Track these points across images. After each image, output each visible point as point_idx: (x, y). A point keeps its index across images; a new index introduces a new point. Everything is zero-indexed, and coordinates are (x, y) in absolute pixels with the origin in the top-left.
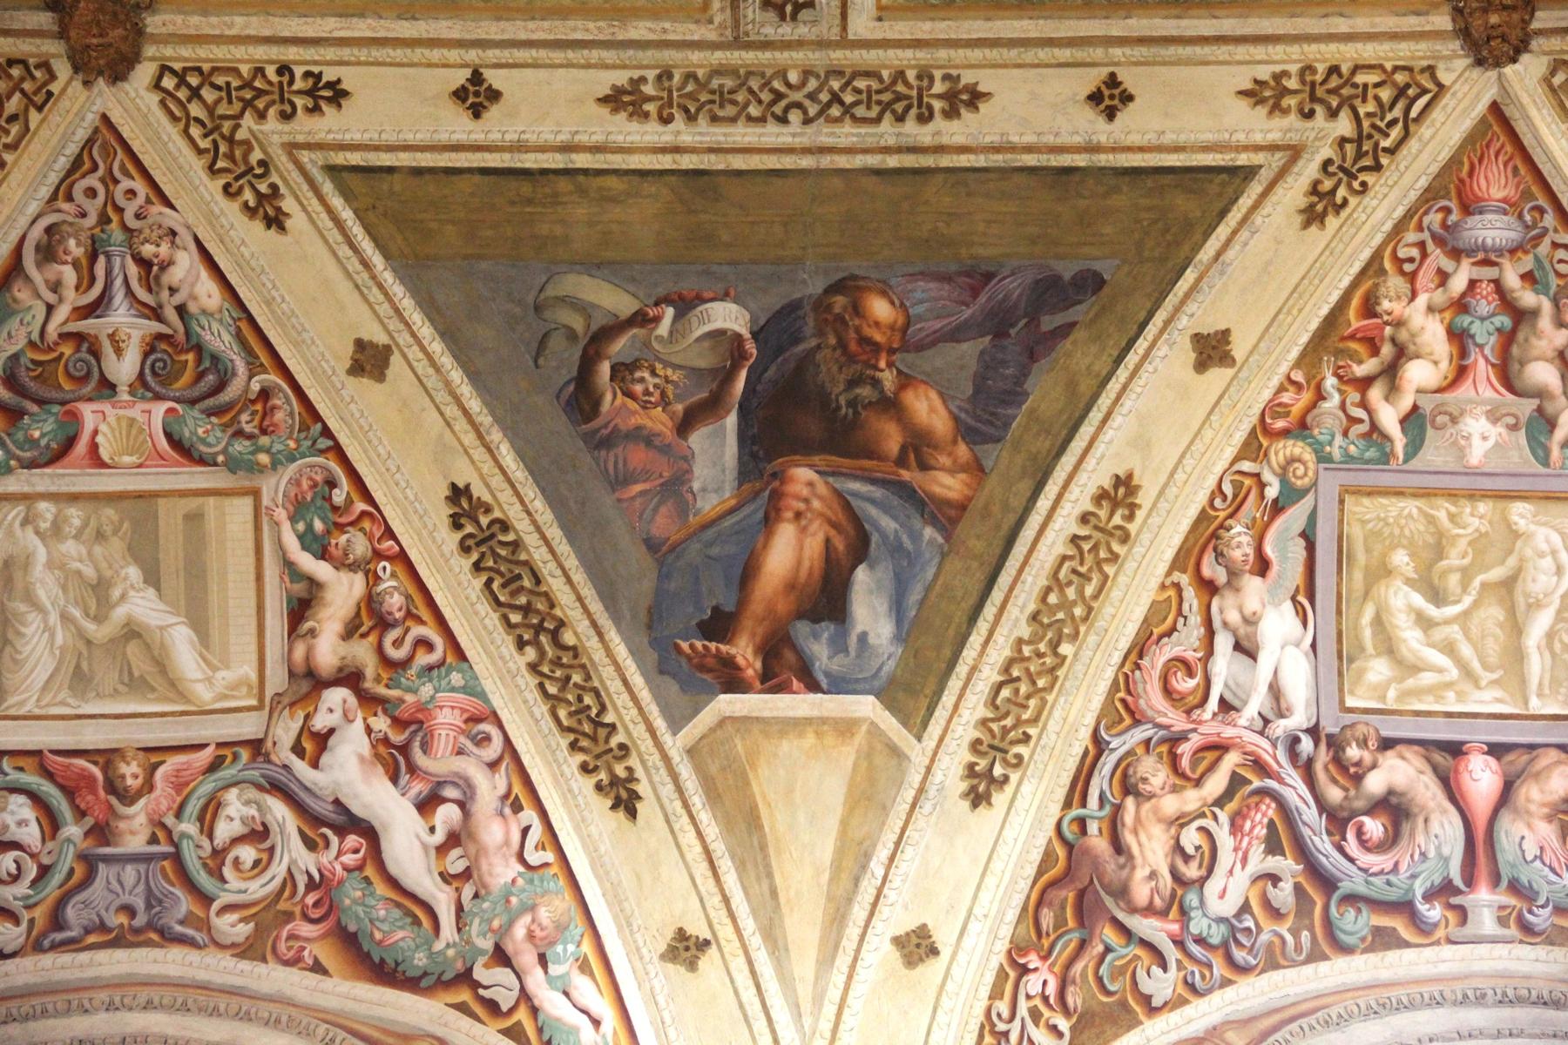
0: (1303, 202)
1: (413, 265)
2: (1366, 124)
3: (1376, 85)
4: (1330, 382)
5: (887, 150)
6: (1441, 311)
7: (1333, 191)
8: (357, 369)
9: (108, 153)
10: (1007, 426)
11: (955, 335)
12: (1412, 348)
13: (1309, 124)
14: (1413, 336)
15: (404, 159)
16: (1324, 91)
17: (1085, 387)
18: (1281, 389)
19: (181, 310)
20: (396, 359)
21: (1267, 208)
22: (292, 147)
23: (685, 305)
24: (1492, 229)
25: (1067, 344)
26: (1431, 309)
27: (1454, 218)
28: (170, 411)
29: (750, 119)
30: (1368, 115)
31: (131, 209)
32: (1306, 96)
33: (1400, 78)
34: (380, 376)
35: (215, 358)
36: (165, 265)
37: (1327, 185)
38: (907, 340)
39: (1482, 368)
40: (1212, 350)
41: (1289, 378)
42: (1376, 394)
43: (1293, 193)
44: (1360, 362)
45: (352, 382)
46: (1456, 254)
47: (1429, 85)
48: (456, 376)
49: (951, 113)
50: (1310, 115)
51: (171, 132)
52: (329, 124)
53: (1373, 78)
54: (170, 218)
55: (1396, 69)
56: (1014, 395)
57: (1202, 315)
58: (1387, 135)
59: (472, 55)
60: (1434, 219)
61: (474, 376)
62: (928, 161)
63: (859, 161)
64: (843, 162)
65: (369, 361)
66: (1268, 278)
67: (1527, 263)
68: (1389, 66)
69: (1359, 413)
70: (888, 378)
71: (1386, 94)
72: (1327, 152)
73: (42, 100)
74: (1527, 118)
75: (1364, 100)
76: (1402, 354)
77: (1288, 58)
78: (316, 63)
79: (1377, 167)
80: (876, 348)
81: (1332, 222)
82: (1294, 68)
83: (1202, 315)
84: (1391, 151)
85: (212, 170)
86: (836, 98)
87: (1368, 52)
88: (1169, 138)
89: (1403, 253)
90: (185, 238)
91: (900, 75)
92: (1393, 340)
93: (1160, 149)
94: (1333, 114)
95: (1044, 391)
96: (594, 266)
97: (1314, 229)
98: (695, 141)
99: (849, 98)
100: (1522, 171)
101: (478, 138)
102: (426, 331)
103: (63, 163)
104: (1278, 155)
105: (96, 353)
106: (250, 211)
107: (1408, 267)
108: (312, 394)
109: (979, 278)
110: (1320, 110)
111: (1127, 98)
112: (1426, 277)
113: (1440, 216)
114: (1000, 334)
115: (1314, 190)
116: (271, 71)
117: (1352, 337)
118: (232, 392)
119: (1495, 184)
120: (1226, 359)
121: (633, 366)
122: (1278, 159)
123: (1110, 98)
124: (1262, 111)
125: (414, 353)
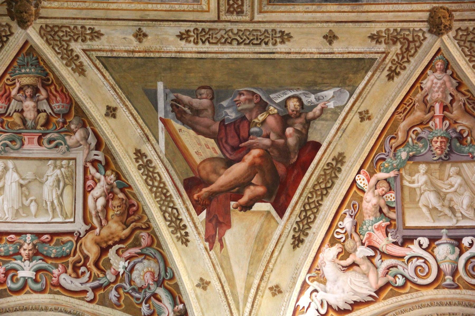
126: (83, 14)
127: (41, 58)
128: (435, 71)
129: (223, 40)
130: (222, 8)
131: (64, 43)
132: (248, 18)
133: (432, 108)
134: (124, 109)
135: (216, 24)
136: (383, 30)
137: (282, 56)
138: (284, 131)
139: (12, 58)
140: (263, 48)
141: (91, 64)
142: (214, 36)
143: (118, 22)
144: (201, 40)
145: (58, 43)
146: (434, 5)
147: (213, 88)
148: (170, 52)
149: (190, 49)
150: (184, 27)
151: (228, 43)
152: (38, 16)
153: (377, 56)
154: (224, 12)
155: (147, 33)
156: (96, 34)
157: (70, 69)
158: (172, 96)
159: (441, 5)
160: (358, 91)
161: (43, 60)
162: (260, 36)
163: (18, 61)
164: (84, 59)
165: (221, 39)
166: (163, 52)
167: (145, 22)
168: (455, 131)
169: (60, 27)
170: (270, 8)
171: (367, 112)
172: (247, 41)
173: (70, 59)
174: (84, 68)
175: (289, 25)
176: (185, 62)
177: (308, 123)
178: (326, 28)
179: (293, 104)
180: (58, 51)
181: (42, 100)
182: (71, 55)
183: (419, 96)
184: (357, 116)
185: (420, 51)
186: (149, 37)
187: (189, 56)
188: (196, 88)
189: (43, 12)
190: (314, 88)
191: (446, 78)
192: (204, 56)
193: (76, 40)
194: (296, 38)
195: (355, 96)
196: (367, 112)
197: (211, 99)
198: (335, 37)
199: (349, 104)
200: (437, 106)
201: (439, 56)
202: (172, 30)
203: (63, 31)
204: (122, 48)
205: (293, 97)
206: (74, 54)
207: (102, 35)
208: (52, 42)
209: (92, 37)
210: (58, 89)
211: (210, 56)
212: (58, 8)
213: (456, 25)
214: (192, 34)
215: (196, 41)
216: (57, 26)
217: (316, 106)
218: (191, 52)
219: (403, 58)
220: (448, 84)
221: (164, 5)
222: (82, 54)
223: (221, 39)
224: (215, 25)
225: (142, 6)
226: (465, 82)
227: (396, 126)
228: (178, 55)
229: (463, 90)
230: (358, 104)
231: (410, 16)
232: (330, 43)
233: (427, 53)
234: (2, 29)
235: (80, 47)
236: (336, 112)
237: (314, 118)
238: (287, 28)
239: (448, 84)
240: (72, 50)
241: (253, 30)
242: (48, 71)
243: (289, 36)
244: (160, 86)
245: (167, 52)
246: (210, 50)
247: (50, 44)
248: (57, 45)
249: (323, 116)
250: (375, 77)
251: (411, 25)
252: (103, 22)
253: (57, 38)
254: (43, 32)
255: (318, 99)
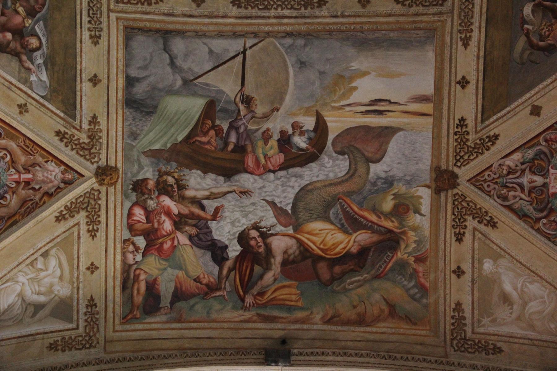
1: (509, 99)
8: (538, 115)
9: (478, 181)
15: (480, 102)
19: (522, 164)
20: (536, 104)
22: (476, 132)
23: (524, 21)
28: (552, 168)
29: (473, 7)
31: (493, 176)
34: (541, 108)
35: (536, 155)
36: (509, 167)
45: (542, 116)
48: (541, 86)
51: (472, 164)
52: (470, 122)
54: (496, 165)
59: (453, 84)
61: (542, 81)
65: (536, 111)
73: (463, 197)
78: (454, 125)
85: (482, 153)
90: (501, 162)
96: (512, 48)
98: (478, 22)
101: (474, 82)
102: (528, 95)
103: (480, 193)
105: (535, 188)
106: (494, 144)
108: (545, 127)
116: (456, 137)
118: (546, 150)
121: (540, 35)
125: (534, 98)
128: (63, 173)
132: (112, 7)
133: (27, 171)
136: (101, 127)
137: (78, 35)
138: (9, 30)
140: (85, 19)
146: (121, 170)
153: (78, 122)
159: (120, 176)
160: (46, 103)
162: (97, 17)
168: (6, 192)
170: (121, 28)
171: (27, 111)
172: (91, 5)
175: (106, 43)
177: (16, 55)
178: (103, 76)
179: (33, 42)
183: (40, 159)
184: (23, 102)
185: (82, 159)
190: (50, 63)
191: (56, 183)
194: (95, 49)
195: (42, 100)
196: (27, 111)
198: (95, 85)
199: (34, 95)
200: (30, 176)
201: (76, 176)
205: (41, 43)
213: (103, 189)
217: (33, 64)
219: (76, 145)
220: (50, 185)
226: (53, 199)
227: (12, 138)
229: (45, 198)
230: (34, 103)
231: (112, 150)
232: (89, 80)
233: (80, 164)
236: (26, 82)
237: (21, 61)
238: (103, 41)
239: (50, 185)
241: (101, 11)
243: (96, 43)
249: (23, 70)
250: (59, 120)
251: (104, 151)
255: (39, 66)
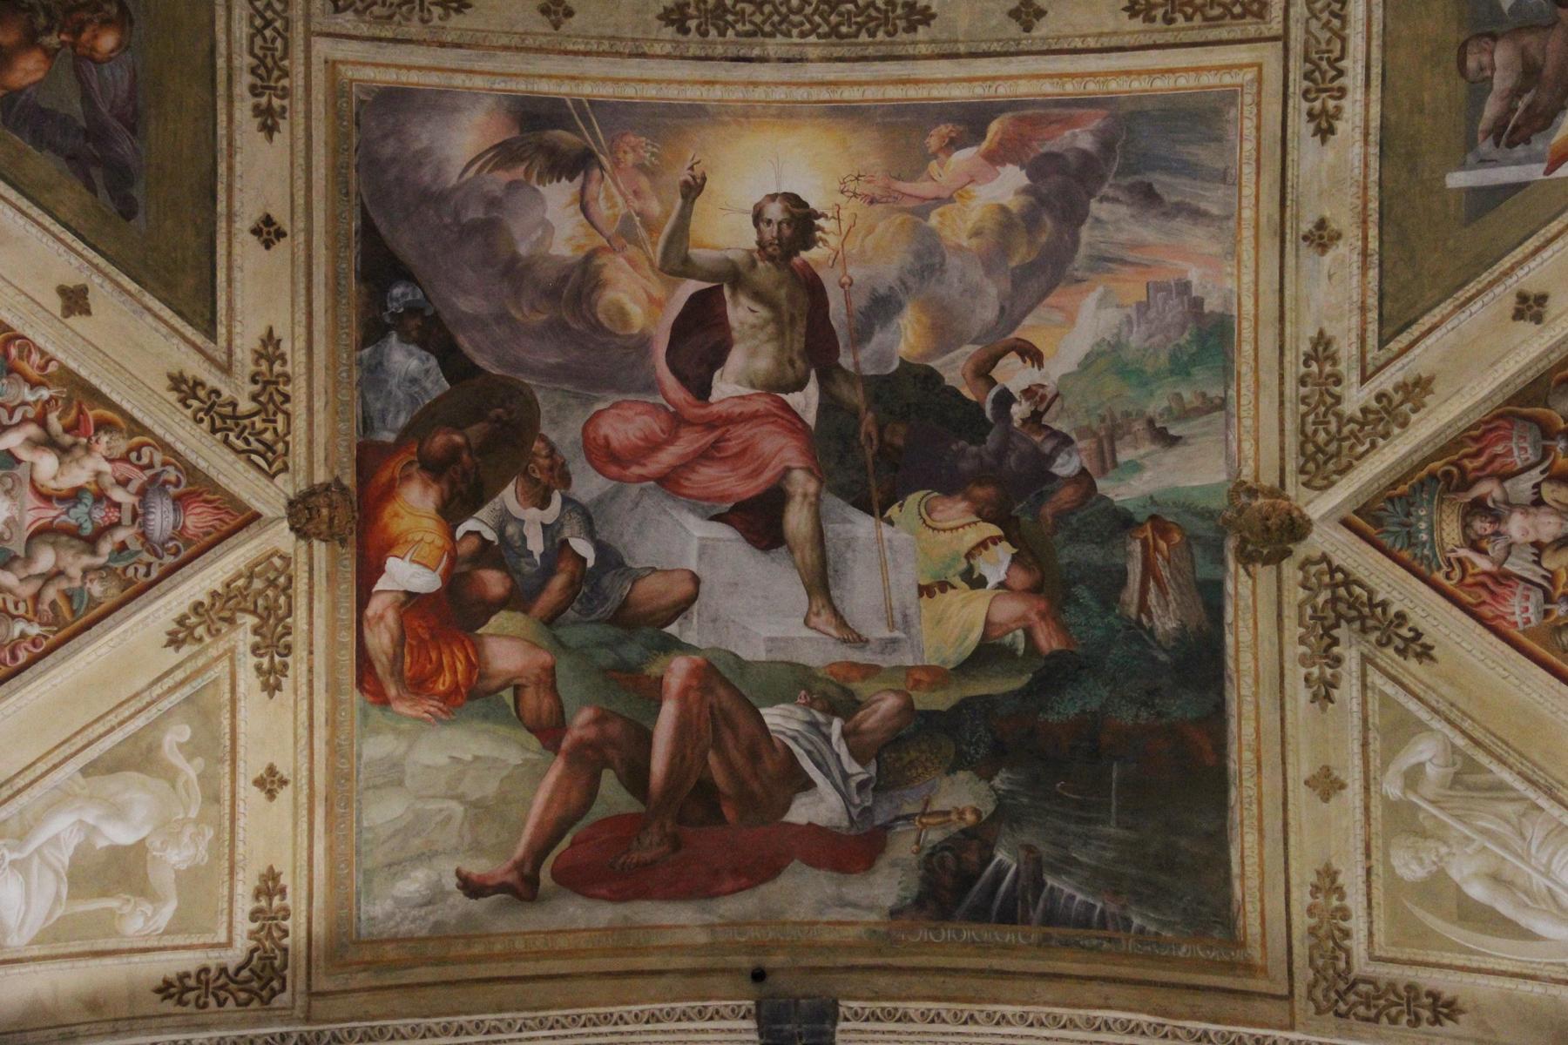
0: (188, 374)
2: (247, 422)
3: (275, 430)
4: (45, 394)
5: (229, 59)
6: (96, 482)
7: (196, 397)
10: (16, 130)
11: (87, 97)
12: (68, 459)
13: (247, 379)
14: (77, 461)
16: (271, 390)
17: (46, 197)
18: (43, 353)
21: (184, 347)
24: (161, 519)
25: (79, 186)
26: (98, 474)
27: (172, 490)
30: (253, 424)
32: (268, 377)
33: (280, 447)
37: (202, 393)
38: (83, 59)
39: (50, 513)
40: (75, 300)
41: (52, 359)
42: (33, 430)
43: (195, 367)
44: (60, 418)
46: (142, 493)
47: (275, 468)
49: (258, 112)
50: (254, 381)
53: (280, 426)
55: (287, 444)
56: (39, 140)
57: (102, 294)
58: (238, 438)
60: (171, 474)
62: (221, 89)
63: (221, 37)
64: (220, 25)
66: (129, 348)
67: (134, 545)
68: (289, 438)
69: (17, 417)
70: (52, 40)
71: (268, 436)
72: (226, 393)
74: (252, 538)
75: (264, 421)
76: (63, 451)
77: (296, 363)
79: (214, 431)
80: (77, 33)
81: (173, 397)
82: (288, 369)
83: (102, 294)
84: (226, 441)
86: (268, 23)
87: (300, 424)
88: (237, 275)
89: (146, 451)
91: (285, 74)
92: (75, 444)
93: (230, 268)
94: (254, 398)
95: (43, 165)
97: (168, 382)
99: (268, 33)
100: (208, 539)
104: (224, 357)
107: (133, 455)
109: (133, 124)
110: (257, 388)
111: (268, 245)
112: (124, 469)
113: (173, 478)
114: (87, 134)
115: (198, 383)
117: (81, 412)
119: (197, 520)
120: (68, 311)
122: (222, 357)
123: (268, 232)
124: (257, 345)
126: (1270, 380)
127: (1387, 488)
129: (1336, 23)
130: (1252, 31)
131: (1346, 431)
134: (1520, 273)
135: (1292, 44)
139: (1388, 562)
141: (1398, 364)
142: (1323, 46)
143: (1287, 293)
144: (1333, 79)
145: (1346, 444)
147: (1462, 39)
148: (1366, 157)
149: (1357, 109)
150: (1300, 126)
151: (1342, 9)
152: (1278, 492)
154: (1263, 27)
155: (1316, 219)
156: (1320, 349)
157: (1414, 417)
158: (1486, 146)
161: (1394, 485)
163: (1398, 547)
164: (1387, 381)
165: (1331, 30)
166: (1365, 177)
167: (1288, 224)
169: (1305, 438)
173: (1385, 416)
174: (1410, 380)
176: (1393, 118)
180: (1367, 445)
181: (1505, 492)
182: (1378, 412)
186: (1327, 214)
187: (1375, 110)
188: (1462, 82)
189: (1269, 479)
192: (1376, 70)
193: (1338, 400)
197: (1494, 37)
202: (1309, 156)
203: (1315, 432)
204: (1355, 281)
206: (1374, 405)
207: (1321, 333)
208: (1344, 461)
209: (1327, 358)
210: (1473, 448)
211: (1376, 54)
212: (1257, 441)
214: (1317, 105)
215: (1336, 94)
216: (1302, 446)
218: (1367, 106)
221: (1244, 178)
222: (1374, 386)
223: (1331, 30)
224: (1296, 47)
225: (1247, 233)
228: (1374, 137)
234: (1314, 580)
235: (1354, 391)
240: (1365, 411)
242: (1424, 473)
244: (1458, 180)
245: (1366, 165)
246: (1361, 56)
247: (1350, 466)
248: (1352, 447)
252: (1288, 330)
253: (1333, 447)
254: (1318, 482)
